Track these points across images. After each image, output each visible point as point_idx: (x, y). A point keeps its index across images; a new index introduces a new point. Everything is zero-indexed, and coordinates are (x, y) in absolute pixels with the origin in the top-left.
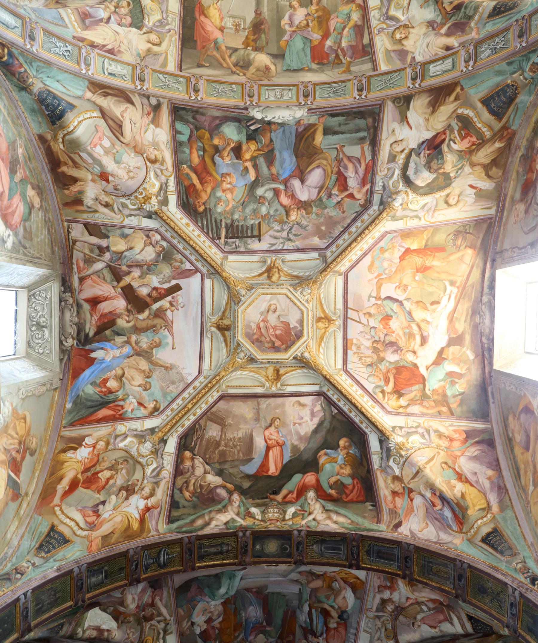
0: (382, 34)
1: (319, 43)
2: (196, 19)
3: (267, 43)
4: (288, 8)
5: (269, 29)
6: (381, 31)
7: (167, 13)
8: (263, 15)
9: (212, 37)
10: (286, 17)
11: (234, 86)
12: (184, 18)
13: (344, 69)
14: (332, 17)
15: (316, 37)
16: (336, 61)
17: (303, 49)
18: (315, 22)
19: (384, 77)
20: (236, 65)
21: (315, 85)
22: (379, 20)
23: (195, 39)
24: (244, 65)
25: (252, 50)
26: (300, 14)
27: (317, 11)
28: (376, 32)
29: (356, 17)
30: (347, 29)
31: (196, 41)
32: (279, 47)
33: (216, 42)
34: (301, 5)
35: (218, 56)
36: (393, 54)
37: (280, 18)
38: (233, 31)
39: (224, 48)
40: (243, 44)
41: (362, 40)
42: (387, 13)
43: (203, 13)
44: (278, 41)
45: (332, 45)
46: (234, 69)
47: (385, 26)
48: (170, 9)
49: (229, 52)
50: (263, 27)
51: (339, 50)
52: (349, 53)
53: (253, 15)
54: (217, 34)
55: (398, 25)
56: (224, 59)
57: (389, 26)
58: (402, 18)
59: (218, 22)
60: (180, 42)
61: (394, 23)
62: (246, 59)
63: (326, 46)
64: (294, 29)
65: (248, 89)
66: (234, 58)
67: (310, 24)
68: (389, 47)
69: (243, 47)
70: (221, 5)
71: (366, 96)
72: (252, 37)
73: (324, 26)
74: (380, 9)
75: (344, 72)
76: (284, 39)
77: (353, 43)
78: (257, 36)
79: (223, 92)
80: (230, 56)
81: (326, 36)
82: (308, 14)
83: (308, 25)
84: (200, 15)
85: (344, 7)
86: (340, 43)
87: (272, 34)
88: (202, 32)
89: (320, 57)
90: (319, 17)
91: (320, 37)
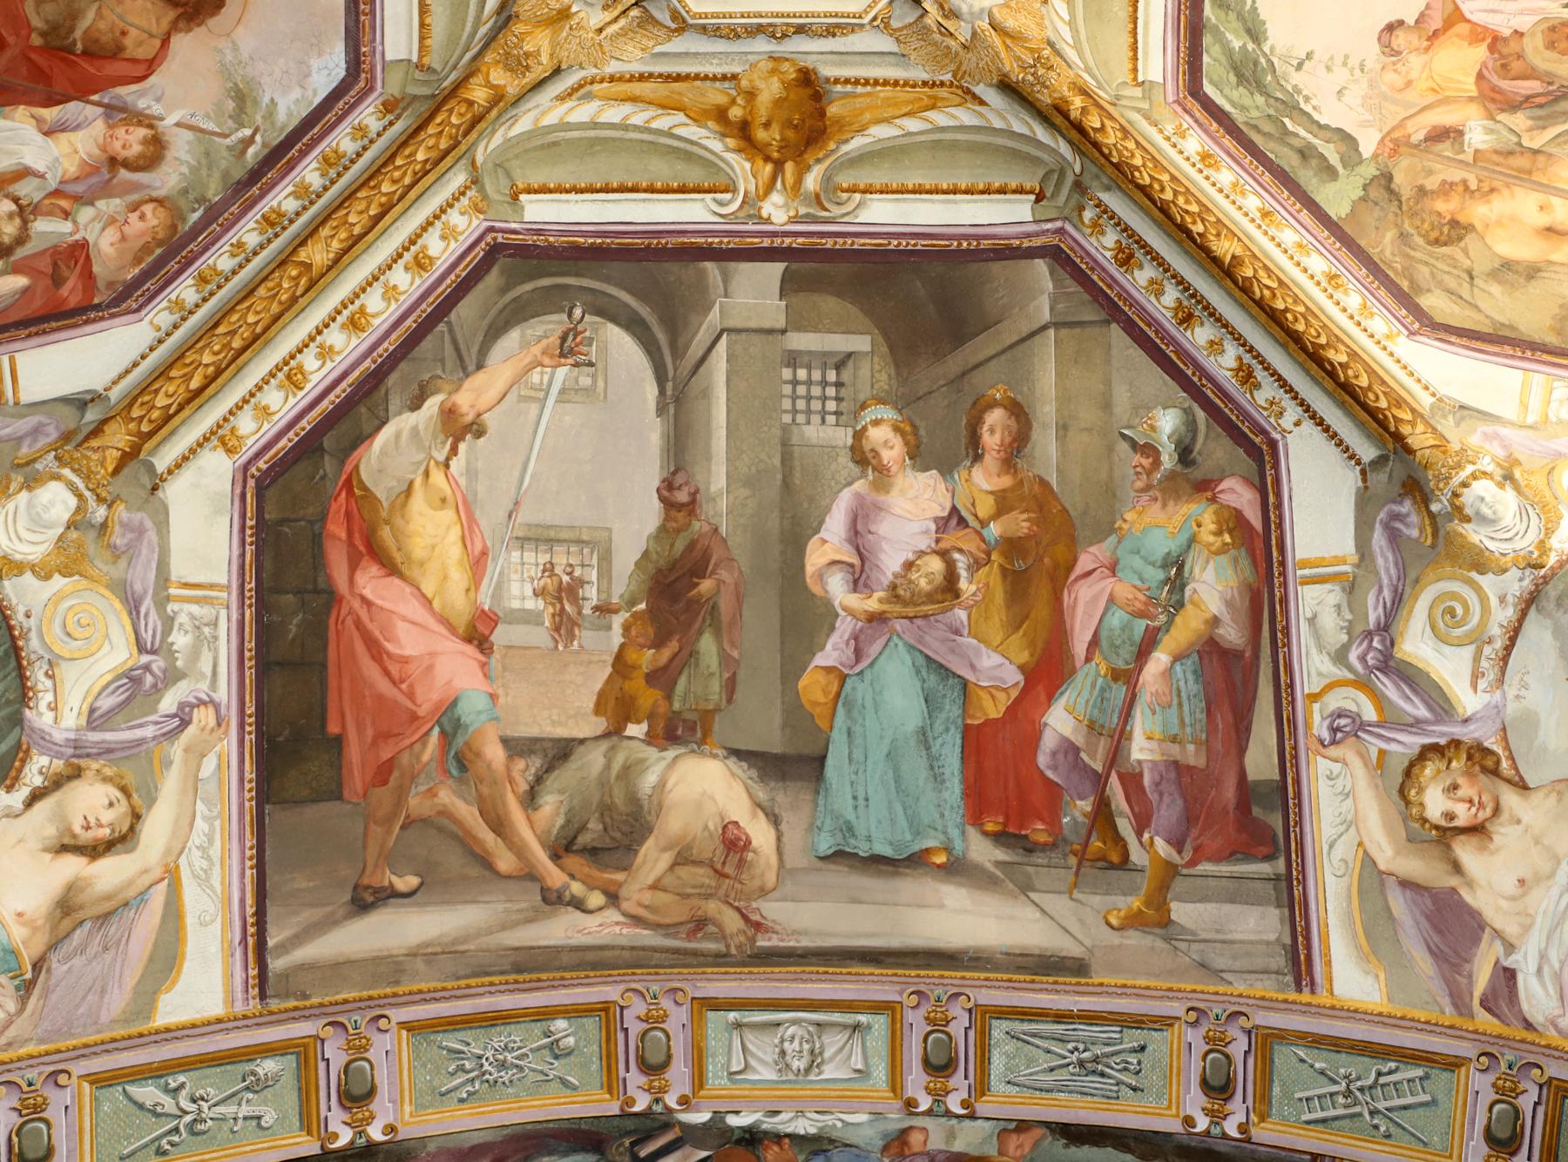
0: (1346, 751)
1: (1012, 710)
2: (331, 598)
3: (731, 686)
4: (844, 459)
5: (739, 599)
6: (1345, 729)
7: (162, 601)
8: (706, 510)
9: (428, 699)
10: (835, 527)
11: (561, 1024)
12: (262, 606)
13: (1136, 903)
14: (1085, 562)
15: (996, 668)
16: (1096, 844)
17: (924, 737)
18: (991, 574)
19: (1347, 1065)
20: (563, 847)
21: (983, 1016)
22: (1340, 657)
23: (333, 728)
24: (608, 837)
25: (650, 739)
26: (913, 507)
27: (1003, 503)
28: (1320, 728)
29: (1214, 588)
30: (1160, 659)
31: (338, 742)
32: (795, 713)
33: (449, 722)
34: (918, 456)
35: (467, 813)
36: (1398, 902)
37: (796, 534)
38: (540, 636)
39: (495, 753)
40: (599, 709)
41: (1242, 750)
42: (1387, 629)
43: (372, 549)
44: (792, 668)
45: (1079, 741)
46: (555, 876)
47: (1370, 713)
48: (180, 568)
49: (524, 770)
50: (706, 585)
51: (1114, 780)
52: (1168, 811)
53: (647, 515)
54: (455, 672)
55: (1440, 734)
56: (499, 825)
57: (1391, 720)
58: (1468, 700)
59: (455, 595)
60: (250, 774)
61: (1422, 712)
62: (619, 798)
63: (1048, 742)
64: (873, 604)
65: (635, 1028)
66: (551, 806)
67: (963, 584)
68: (1386, 854)
69: (599, 725)
70: (471, 473)
71: (1243, 1128)
72: (647, 659)
73: (1041, 611)
74: (1351, 587)
75: (1134, 921)
76: (820, 660)
77: (1192, 755)
78: (673, 646)
79: (502, 1065)
80: (531, 799)
81: (1047, 672)
82: (954, 519)
83: (949, 587)
84: (353, 567)
85: (1155, 513)
86: (1121, 737)
87: (759, 624)
88: (371, 670)
89: (1011, 797)
90: (1012, 546)
91: (1013, 677)
